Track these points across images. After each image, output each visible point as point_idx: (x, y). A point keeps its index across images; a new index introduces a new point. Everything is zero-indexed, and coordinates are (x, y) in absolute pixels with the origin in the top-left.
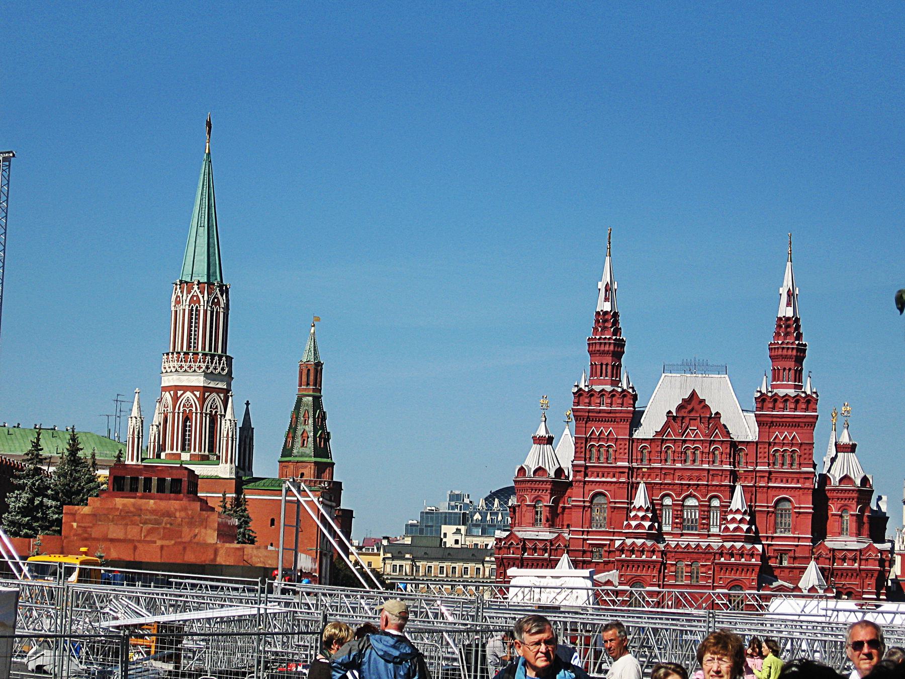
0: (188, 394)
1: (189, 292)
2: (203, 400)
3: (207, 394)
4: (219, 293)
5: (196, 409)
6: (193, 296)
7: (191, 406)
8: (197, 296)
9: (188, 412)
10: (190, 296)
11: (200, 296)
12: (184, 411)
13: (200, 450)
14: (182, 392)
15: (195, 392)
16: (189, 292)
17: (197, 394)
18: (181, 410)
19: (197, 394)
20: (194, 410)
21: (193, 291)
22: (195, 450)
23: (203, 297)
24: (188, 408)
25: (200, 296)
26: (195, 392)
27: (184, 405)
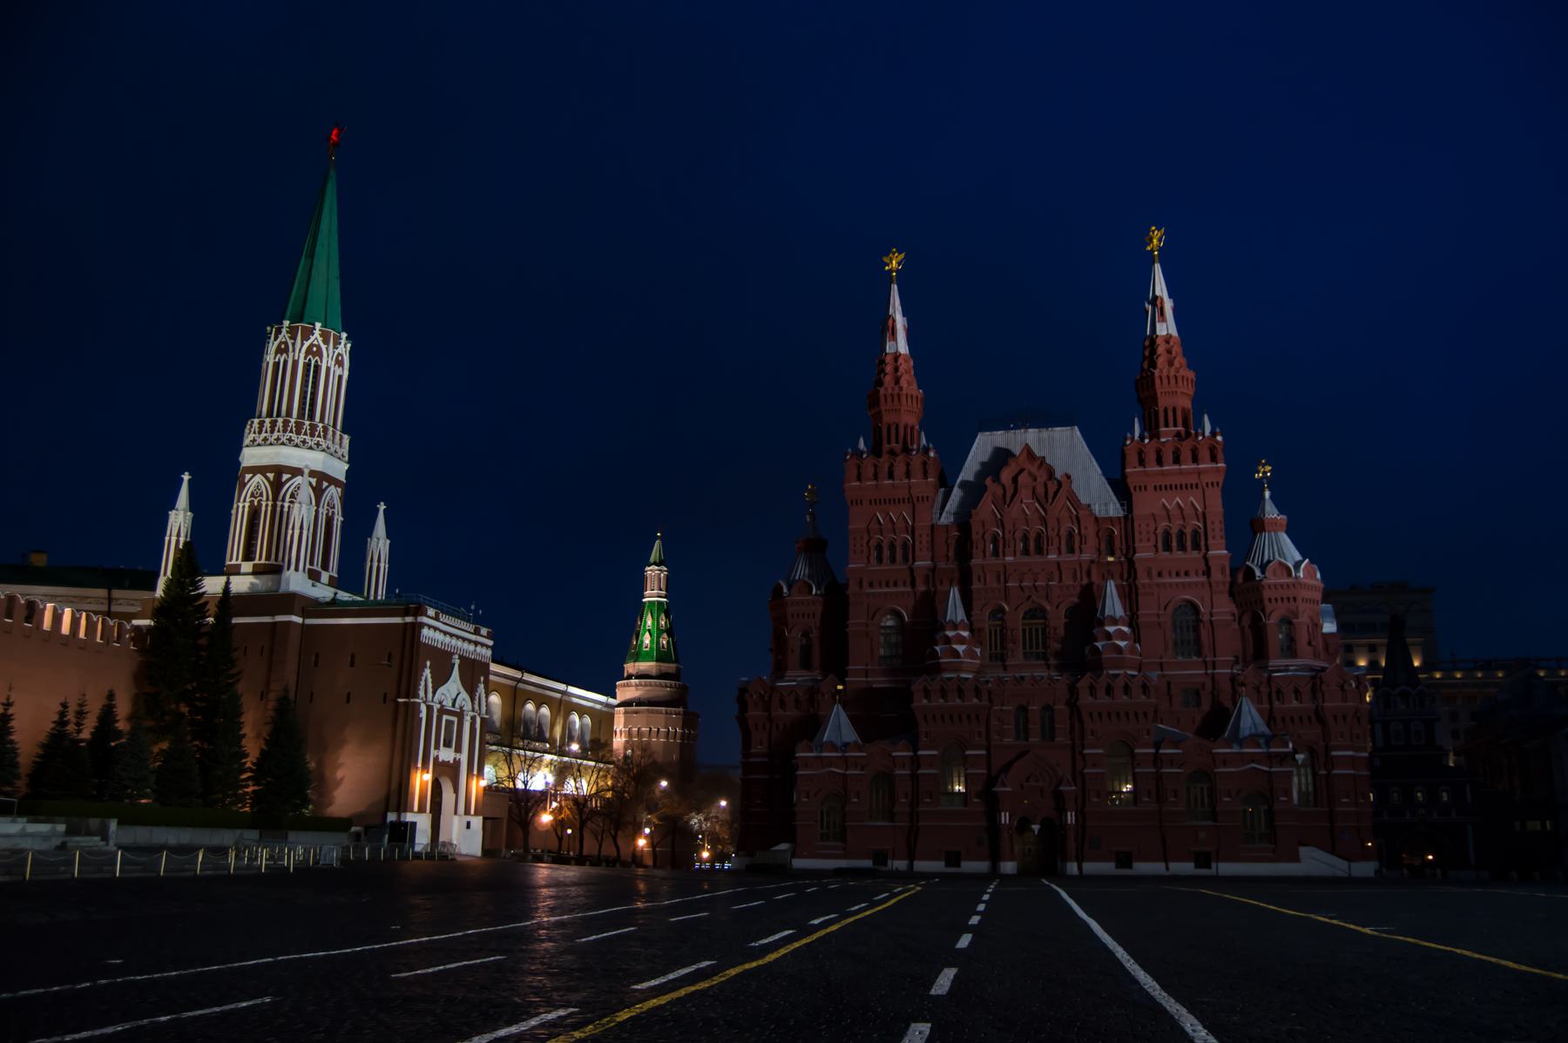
0: (259, 478)
1: (275, 340)
2: (277, 486)
3: (285, 477)
4: (320, 339)
5: (267, 499)
6: (281, 343)
7: (261, 495)
8: (286, 343)
9: (256, 504)
10: (277, 343)
11: (290, 342)
12: (252, 502)
13: (268, 558)
14: (251, 475)
15: (268, 474)
16: (276, 339)
17: (271, 476)
18: (248, 500)
19: (271, 476)
20: (265, 498)
21: (281, 337)
22: (260, 558)
23: (294, 344)
24: (256, 498)
25: (290, 342)
26: (268, 474)
27: (252, 495)
